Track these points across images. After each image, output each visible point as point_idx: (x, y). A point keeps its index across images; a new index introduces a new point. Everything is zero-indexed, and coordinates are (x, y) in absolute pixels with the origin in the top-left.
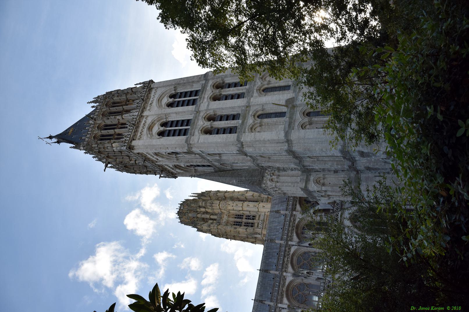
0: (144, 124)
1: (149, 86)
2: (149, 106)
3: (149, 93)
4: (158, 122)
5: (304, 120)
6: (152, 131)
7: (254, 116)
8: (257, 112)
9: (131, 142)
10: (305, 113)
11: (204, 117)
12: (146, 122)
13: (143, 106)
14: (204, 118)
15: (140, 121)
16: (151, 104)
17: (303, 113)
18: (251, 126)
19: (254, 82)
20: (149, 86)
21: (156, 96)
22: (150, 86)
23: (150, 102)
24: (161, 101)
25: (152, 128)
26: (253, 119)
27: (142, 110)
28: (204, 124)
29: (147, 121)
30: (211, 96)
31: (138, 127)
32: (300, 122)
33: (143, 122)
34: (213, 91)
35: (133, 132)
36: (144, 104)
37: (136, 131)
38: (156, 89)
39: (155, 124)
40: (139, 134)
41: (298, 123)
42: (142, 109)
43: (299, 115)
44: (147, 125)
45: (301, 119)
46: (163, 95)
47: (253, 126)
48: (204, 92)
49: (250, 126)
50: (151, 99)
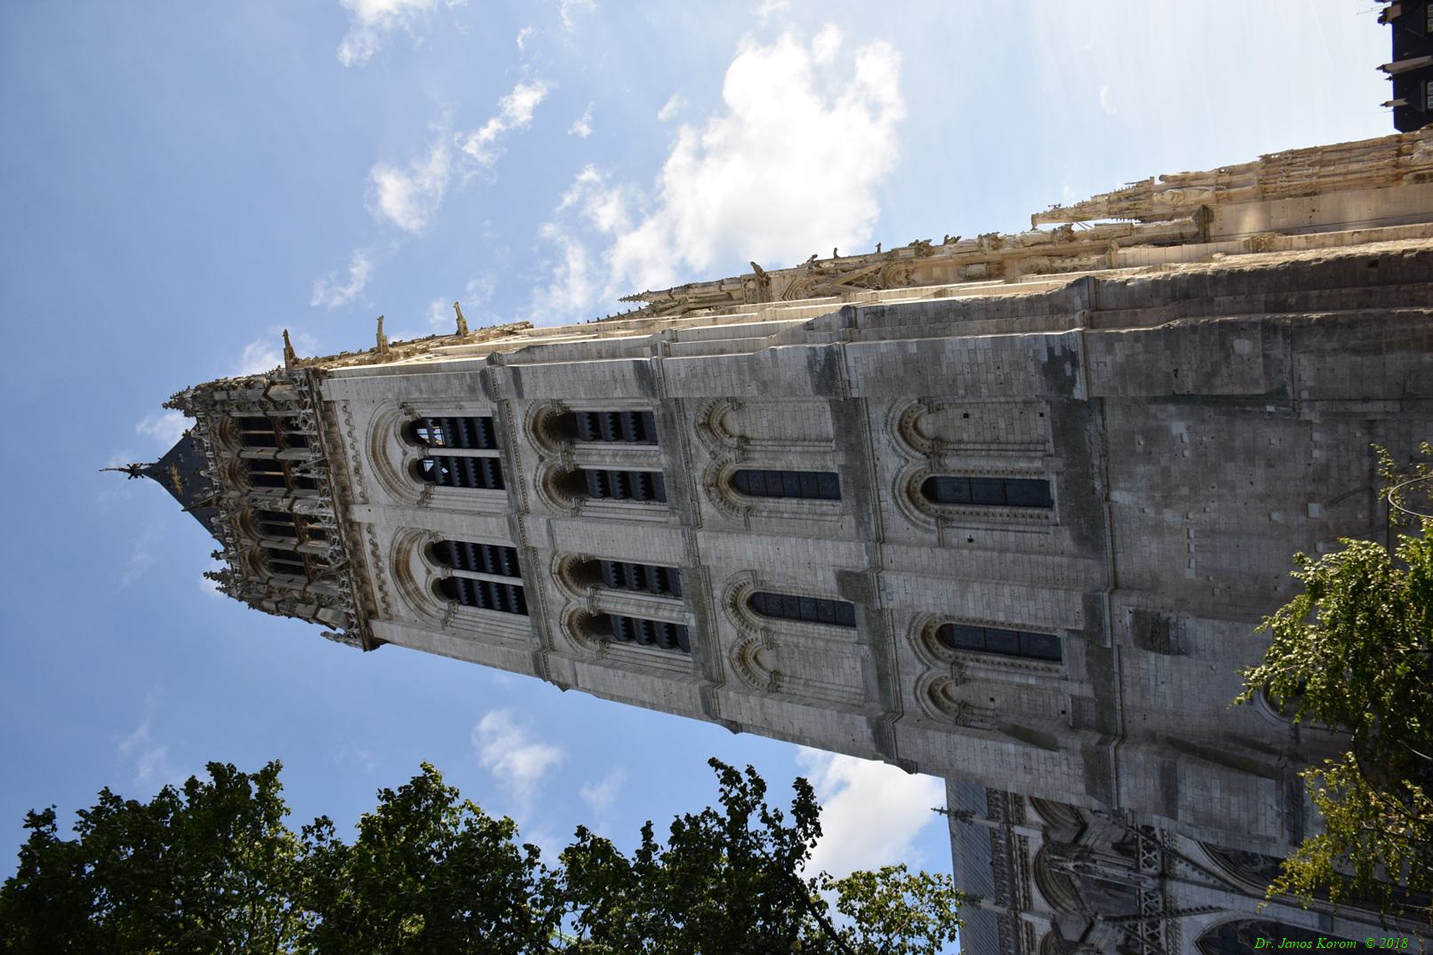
0: (373, 553)
1: (315, 397)
2: (355, 479)
3: (331, 425)
4: (415, 545)
5: (934, 670)
6: (411, 578)
7: (734, 605)
8: (738, 589)
9: (367, 624)
10: (933, 632)
11: (555, 569)
12: (375, 545)
13: (337, 483)
14: (560, 573)
15: (356, 544)
16: (357, 470)
17: (925, 635)
18: (736, 649)
19: (684, 447)
20: (315, 397)
21: (356, 433)
22: (319, 394)
23: (352, 464)
24: (384, 453)
25: (407, 563)
26: (735, 620)
27: (341, 504)
28: (568, 602)
29: (378, 540)
30: (546, 475)
31: (361, 564)
32: (921, 676)
33: (368, 548)
34: (541, 459)
35: (355, 591)
36: (337, 475)
37: (364, 581)
38: (343, 404)
39: (409, 552)
40: (378, 595)
41: (914, 679)
42: (339, 497)
43: (905, 642)
44: (386, 563)
45: (919, 668)
46: (379, 444)
47: (744, 648)
48: (513, 458)
49: (731, 650)
50: (350, 453)
